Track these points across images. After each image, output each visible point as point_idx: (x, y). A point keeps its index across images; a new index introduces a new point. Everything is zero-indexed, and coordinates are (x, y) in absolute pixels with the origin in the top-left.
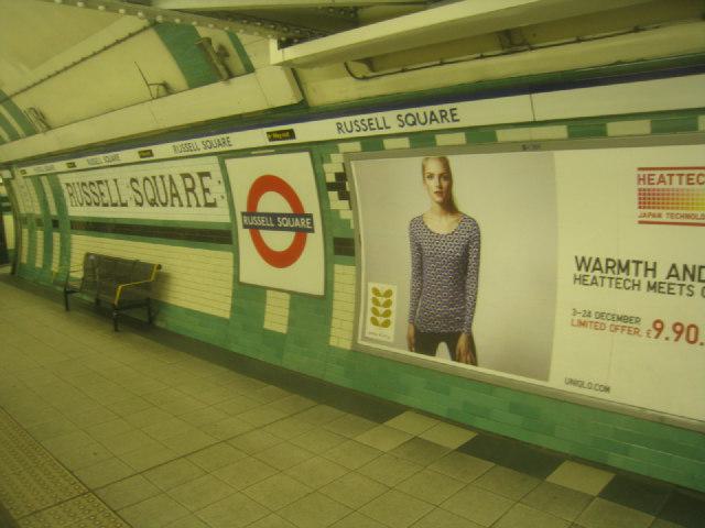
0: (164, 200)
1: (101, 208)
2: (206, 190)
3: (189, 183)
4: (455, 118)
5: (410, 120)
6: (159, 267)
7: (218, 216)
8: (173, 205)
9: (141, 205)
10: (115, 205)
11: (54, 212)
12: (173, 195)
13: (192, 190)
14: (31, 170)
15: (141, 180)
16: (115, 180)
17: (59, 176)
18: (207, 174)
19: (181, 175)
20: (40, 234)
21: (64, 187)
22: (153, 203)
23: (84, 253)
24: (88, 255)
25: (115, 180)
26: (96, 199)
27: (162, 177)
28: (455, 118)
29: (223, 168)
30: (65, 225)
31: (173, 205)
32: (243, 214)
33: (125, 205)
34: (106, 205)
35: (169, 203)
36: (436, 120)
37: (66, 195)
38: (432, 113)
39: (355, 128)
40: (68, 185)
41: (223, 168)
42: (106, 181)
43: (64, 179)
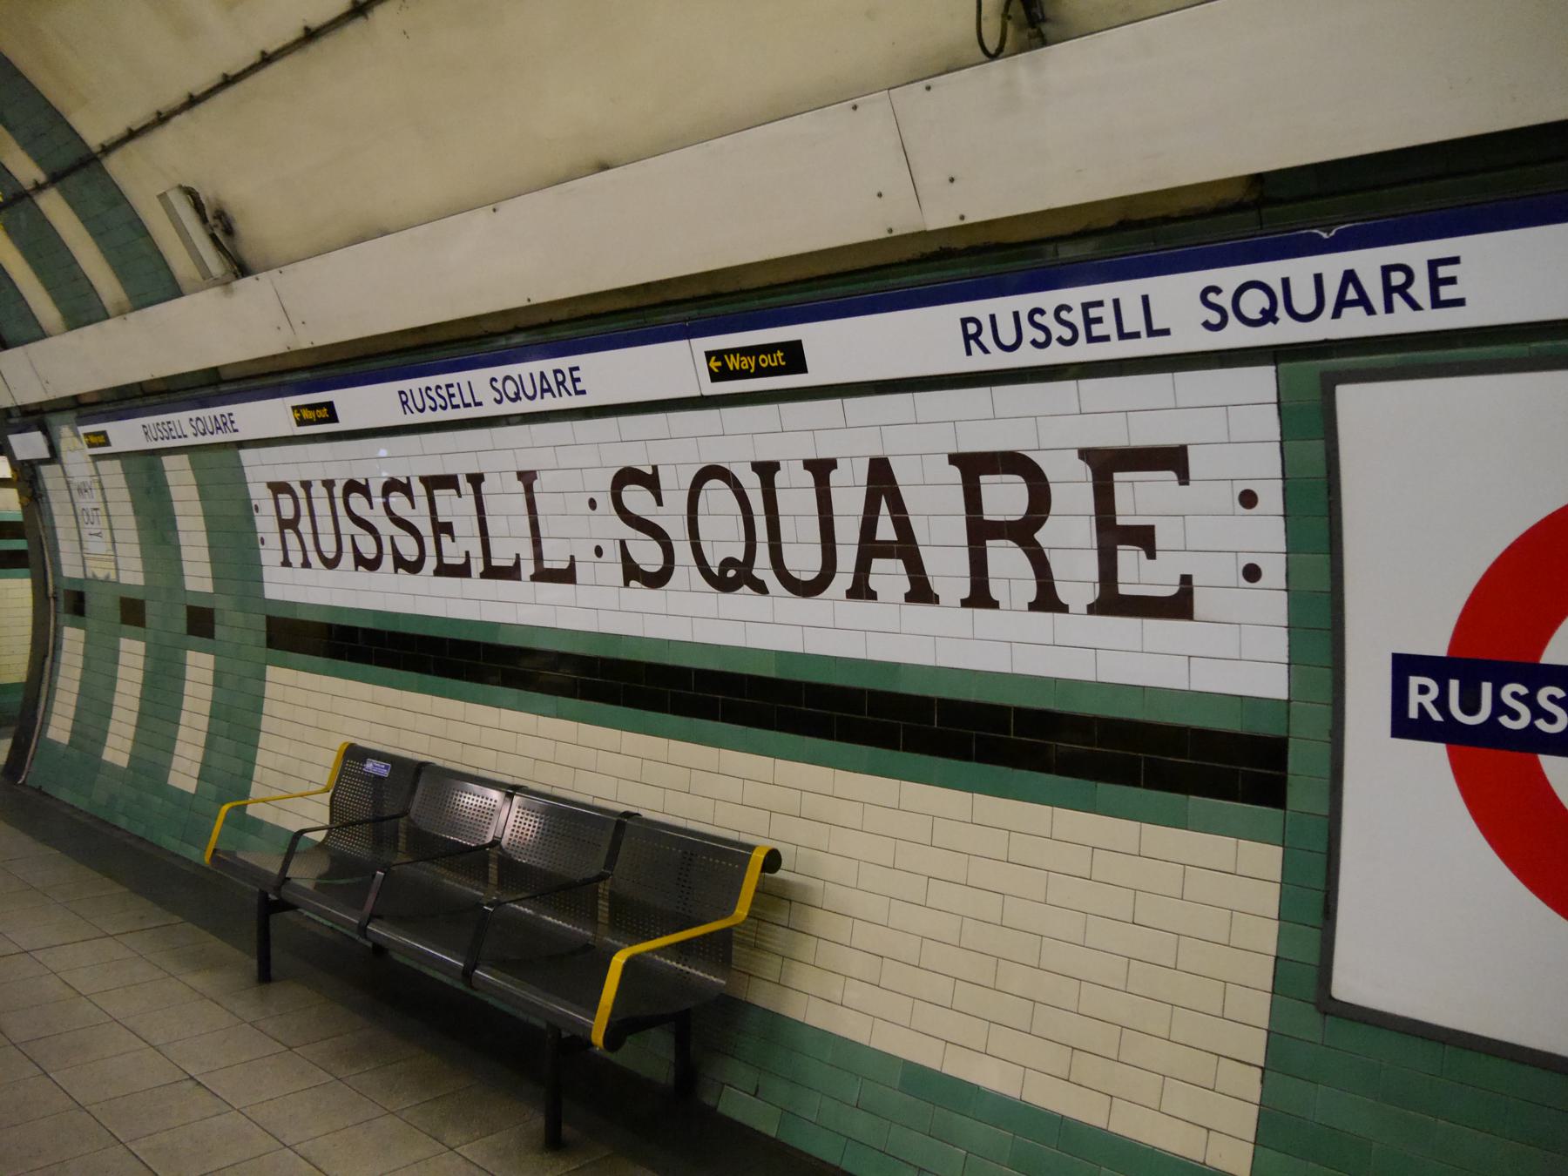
0: (804, 560)
1: (475, 585)
2: (1114, 536)
3: (1005, 497)
6: (773, 860)
7: (1231, 656)
8: (861, 590)
9: (657, 580)
10: (512, 573)
11: (198, 577)
12: (870, 549)
13: (1023, 532)
14: (127, 434)
15: (675, 485)
16: (527, 478)
17: (246, 455)
18: (1173, 460)
19: (954, 459)
20: (132, 653)
21: (259, 494)
22: (731, 577)
23: (338, 743)
24: (354, 754)
25: (527, 478)
26: (409, 549)
27: (821, 469)
29: (1310, 432)
30: (235, 625)
31: (861, 590)
32: (1404, 666)
33: (567, 576)
34: (462, 571)
35: (843, 579)
37: (266, 524)
40: (278, 488)
41: (1310, 432)
42: (476, 480)
43: (259, 468)
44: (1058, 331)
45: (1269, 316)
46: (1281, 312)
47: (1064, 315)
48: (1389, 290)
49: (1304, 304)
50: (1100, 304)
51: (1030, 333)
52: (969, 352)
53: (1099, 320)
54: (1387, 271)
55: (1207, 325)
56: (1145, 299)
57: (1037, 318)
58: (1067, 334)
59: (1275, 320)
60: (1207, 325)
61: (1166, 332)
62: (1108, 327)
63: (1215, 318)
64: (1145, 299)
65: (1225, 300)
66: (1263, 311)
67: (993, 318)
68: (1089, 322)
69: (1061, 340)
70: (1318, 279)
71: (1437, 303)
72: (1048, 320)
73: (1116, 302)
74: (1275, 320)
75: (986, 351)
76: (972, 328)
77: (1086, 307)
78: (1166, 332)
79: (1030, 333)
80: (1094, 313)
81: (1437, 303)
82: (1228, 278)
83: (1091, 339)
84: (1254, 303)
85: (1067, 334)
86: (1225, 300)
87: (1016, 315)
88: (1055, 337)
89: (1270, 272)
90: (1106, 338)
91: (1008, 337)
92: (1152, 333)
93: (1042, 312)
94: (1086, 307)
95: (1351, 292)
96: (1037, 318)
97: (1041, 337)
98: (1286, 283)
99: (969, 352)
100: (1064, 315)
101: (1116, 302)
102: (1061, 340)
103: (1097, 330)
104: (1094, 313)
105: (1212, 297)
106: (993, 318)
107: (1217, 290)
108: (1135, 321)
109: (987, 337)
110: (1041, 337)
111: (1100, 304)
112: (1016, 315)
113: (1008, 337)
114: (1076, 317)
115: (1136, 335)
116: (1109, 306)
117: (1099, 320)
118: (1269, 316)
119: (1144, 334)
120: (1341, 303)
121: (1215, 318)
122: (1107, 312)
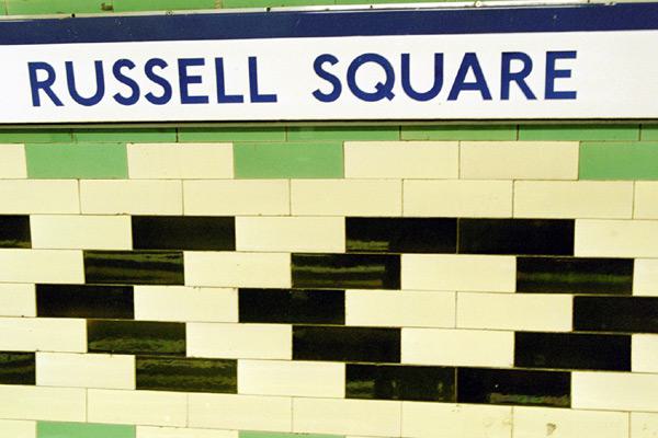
44: (147, 86)
45: (384, 91)
46: (398, 88)
47: (156, 70)
49: (422, 82)
50: (200, 62)
51: (113, 86)
52: (36, 102)
53: (198, 80)
55: (318, 94)
56: (252, 62)
57: (124, 71)
58: (159, 91)
59: (391, 96)
60: (318, 94)
61: (272, 98)
62: (208, 87)
63: (327, 88)
64: (252, 62)
66: (379, 86)
67: (69, 65)
68: (185, 80)
69: (150, 97)
72: (137, 73)
73: (219, 62)
74: (391, 96)
75: (58, 102)
76: (42, 75)
77: (183, 64)
78: (272, 98)
79: (113, 86)
80: (191, 71)
83: (186, 99)
84: (370, 76)
85: (159, 91)
87: (99, 65)
88: (143, 93)
90: (204, 100)
91: (87, 88)
92: (256, 98)
93: (131, 65)
94: (183, 64)
96: (124, 71)
97: (127, 92)
98: (405, 59)
99: (36, 102)
100: (156, 70)
101: (219, 62)
102: (150, 97)
103: (193, 90)
104: (191, 71)
105: (326, 66)
106: (69, 65)
107: (333, 60)
108: (237, 83)
109: (60, 87)
110: (127, 92)
111: (200, 62)
112: (99, 65)
113: (87, 88)
114: (171, 74)
115: (239, 99)
116: (210, 66)
117: (198, 80)
118: (384, 91)
119: (247, 97)
121: (327, 88)
122: (208, 72)
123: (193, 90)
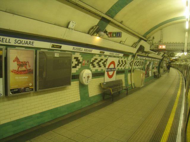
4: (33, 44)
5: (19, 42)
28: (33, 44)
36: (27, 44)
38: (27, 42)
39: (77, 49)
45: (20, 43)
48: (29, 43)
49: (23, 43)
53: (4, 40)
54: (30, 42)
55: (14, 43)
56: (9, 39)
60: (14, 43)
62: (5, 41)
63: (15, 42)
64: (9, 39)
65: (17, 41)
68: (2, 40)
70: (25, 41)
71: (32, 45)
73: (6, 39)
81: (32, 45)
82: (18, 39)
86: (17, 41)
89: (21, 40)
90: (4, 42)
92: (9, 42)
94: (3, 38)
95: (27, 43)
101: (6, 39)
104: (3, 39)
108: (7, 41)
117: (4, 40)
118: (20, 43)
120: (26, 43)
122: (5, 40)
123: (3, 41)
